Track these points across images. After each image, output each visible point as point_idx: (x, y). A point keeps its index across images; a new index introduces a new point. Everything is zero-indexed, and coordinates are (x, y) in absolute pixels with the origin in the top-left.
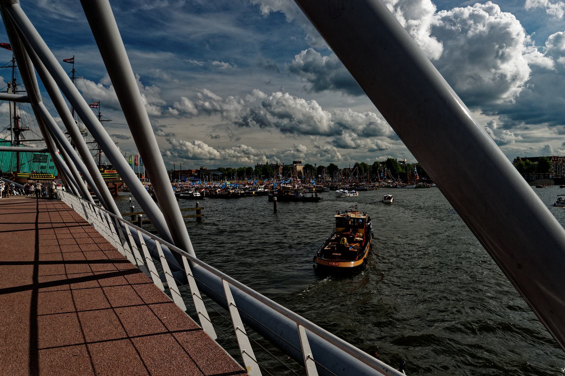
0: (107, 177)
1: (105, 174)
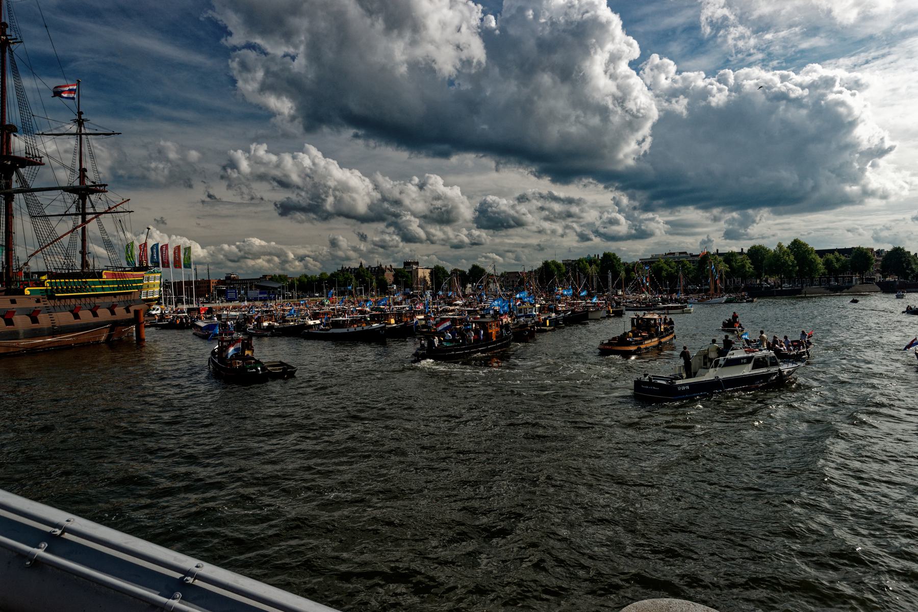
0: (111, 289)
1: (104, 282)
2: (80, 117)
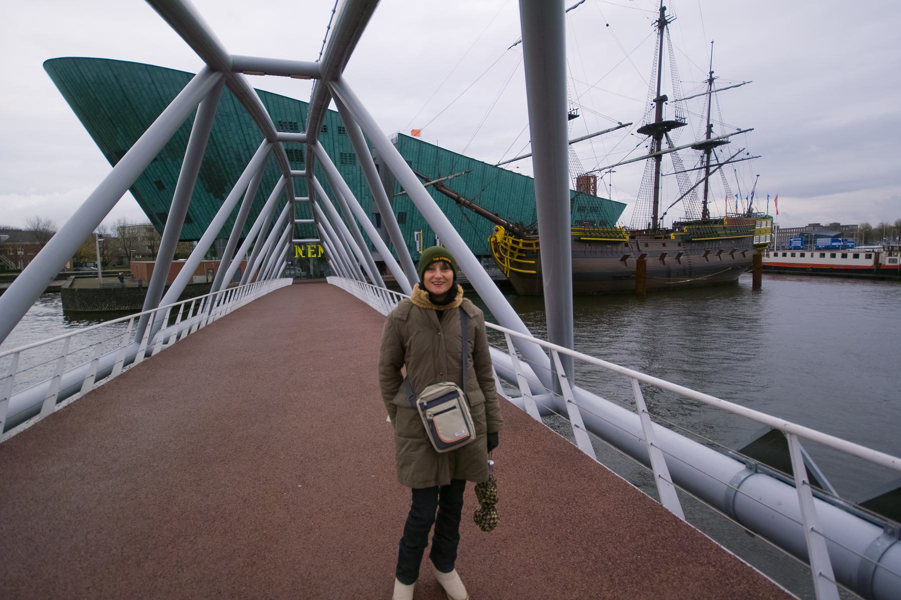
2: (711, 76)
